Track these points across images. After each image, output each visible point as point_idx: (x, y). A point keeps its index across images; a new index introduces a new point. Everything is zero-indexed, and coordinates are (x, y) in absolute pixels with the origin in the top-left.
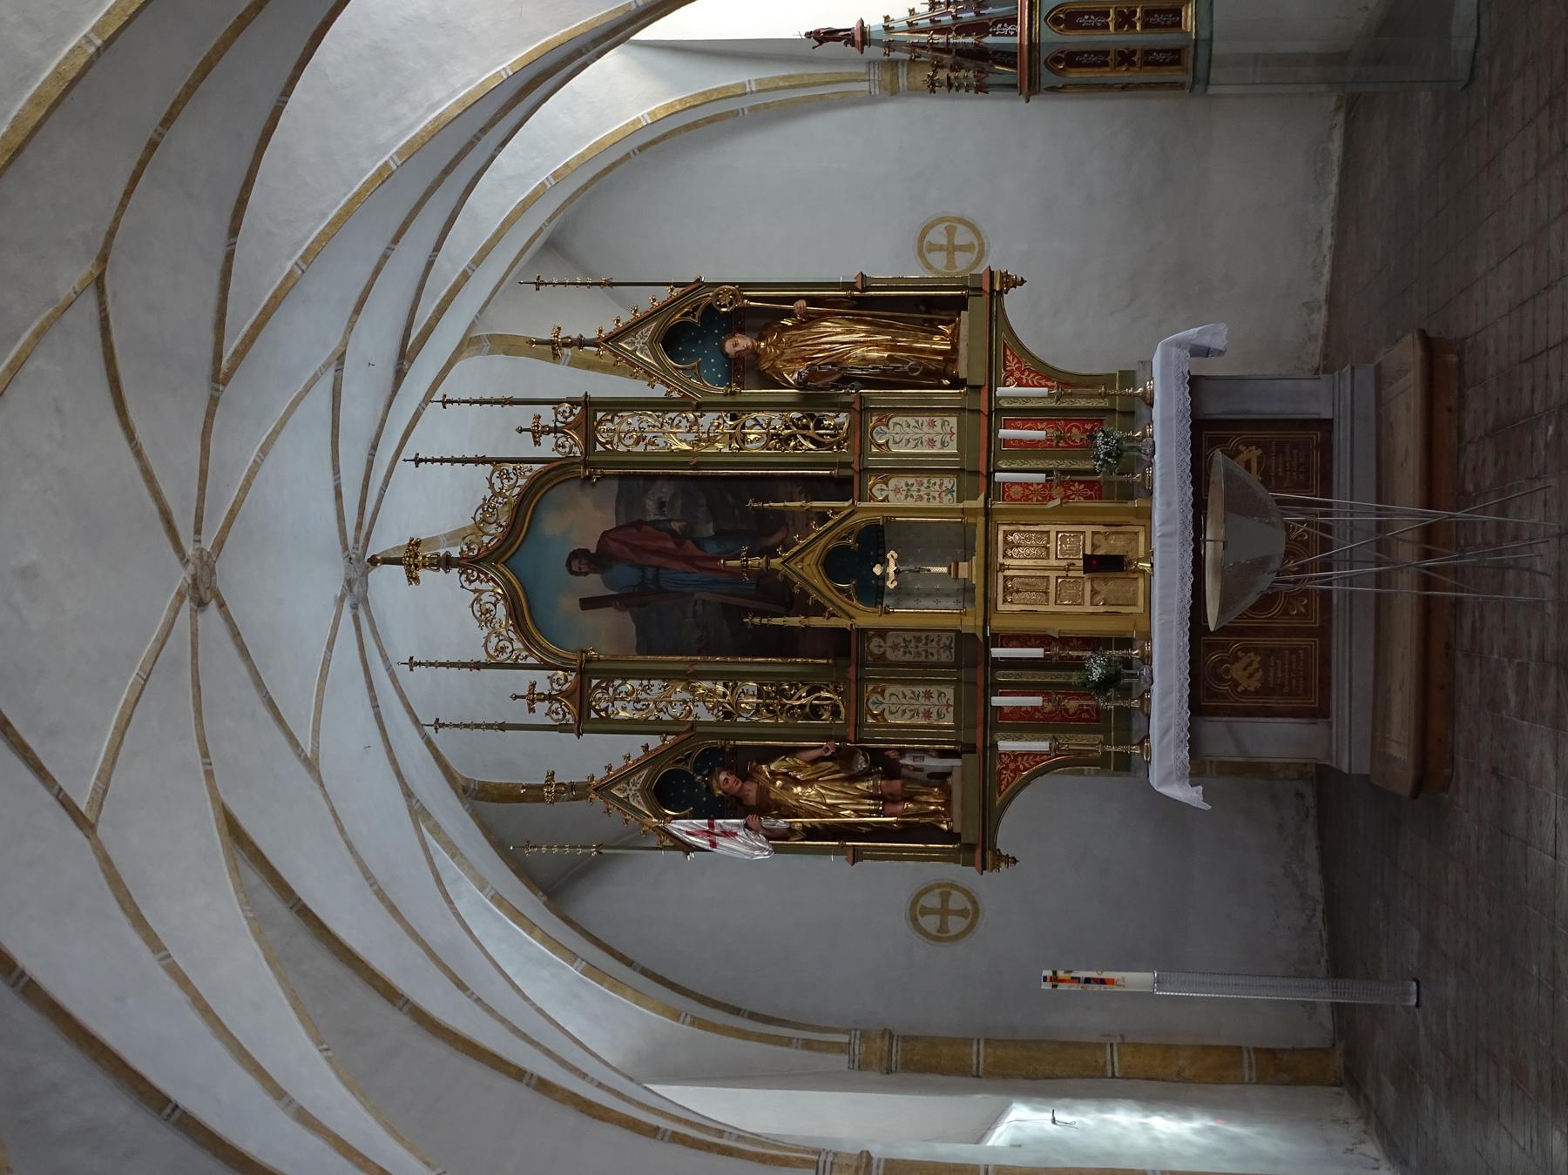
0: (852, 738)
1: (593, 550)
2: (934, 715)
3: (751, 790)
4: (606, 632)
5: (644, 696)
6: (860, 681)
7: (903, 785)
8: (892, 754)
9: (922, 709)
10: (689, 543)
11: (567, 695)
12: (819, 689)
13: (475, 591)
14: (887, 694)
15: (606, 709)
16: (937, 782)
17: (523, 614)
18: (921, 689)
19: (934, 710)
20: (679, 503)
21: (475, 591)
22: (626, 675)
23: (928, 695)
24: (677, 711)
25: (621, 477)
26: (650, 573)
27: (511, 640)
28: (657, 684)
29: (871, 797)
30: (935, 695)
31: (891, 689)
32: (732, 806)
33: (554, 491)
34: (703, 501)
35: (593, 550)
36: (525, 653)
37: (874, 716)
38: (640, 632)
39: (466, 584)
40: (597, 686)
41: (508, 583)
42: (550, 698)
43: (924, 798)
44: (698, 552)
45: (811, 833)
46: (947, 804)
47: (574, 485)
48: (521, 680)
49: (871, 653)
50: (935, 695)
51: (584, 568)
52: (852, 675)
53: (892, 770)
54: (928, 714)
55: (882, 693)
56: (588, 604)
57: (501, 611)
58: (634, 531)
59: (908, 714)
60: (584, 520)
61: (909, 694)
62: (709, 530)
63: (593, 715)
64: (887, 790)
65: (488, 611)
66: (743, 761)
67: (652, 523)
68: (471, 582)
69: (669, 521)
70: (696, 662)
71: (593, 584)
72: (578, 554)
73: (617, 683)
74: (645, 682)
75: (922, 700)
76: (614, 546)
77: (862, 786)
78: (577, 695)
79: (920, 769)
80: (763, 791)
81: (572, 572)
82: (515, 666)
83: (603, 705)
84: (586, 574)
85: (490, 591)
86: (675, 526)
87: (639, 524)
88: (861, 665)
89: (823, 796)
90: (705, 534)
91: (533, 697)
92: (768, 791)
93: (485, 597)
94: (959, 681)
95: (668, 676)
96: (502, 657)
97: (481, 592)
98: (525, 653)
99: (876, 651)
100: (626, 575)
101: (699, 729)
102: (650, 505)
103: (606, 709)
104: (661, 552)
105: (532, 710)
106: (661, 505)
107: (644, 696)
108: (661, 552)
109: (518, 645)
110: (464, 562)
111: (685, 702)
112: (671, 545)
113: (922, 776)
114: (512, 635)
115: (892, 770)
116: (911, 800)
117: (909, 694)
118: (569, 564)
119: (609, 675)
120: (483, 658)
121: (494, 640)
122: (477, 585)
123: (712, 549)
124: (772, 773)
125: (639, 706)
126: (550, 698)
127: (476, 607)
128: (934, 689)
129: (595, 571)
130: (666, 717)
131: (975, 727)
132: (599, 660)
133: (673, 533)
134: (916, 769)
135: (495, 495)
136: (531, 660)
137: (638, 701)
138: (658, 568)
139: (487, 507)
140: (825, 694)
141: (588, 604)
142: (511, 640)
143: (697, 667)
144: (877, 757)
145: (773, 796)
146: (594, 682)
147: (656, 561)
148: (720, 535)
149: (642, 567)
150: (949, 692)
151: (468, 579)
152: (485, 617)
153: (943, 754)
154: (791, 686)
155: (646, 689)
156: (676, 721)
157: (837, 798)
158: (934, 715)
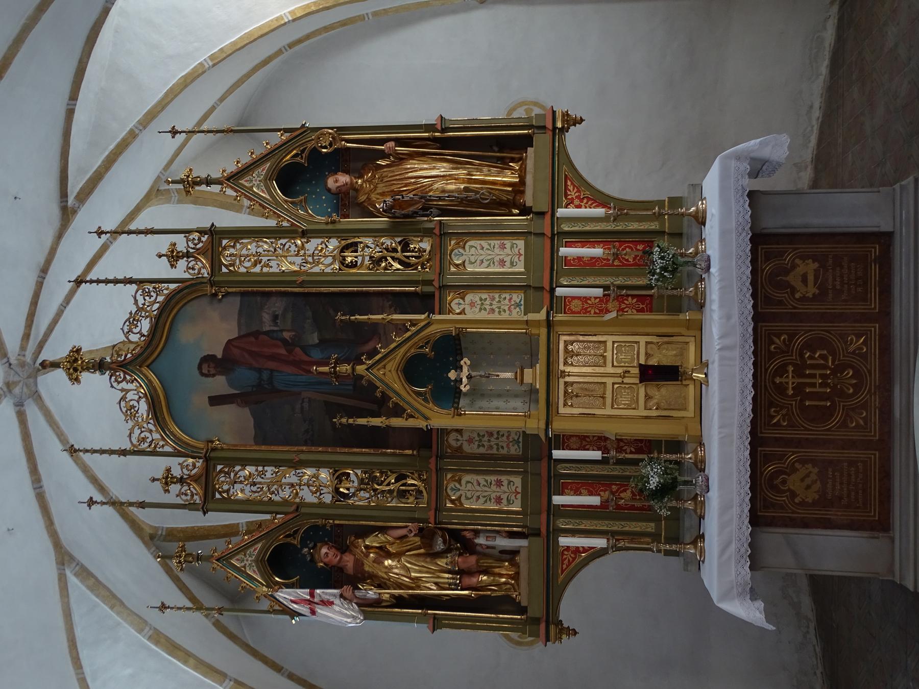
0: (432, 520)
1: (219, 356)
2: (505, 501)
3: (349, 561)
4: (230, 425)
5: (259, 479)
6: (440, 471)
7: (477, 561)
8: (468, 535)
9: (493, 495)
10: (298, 350)
11: (196, 479)
12: (404, 477)
13: (122, 390)
14: (463, 482)
15: (228, 491)
16: (508, 557)
17: (160, 409)
18: (493, 478)
19: (504, 497)
20: (289, 316)
21: (122, 390)
22: (244, 463)
23: (499, 483)
24: (286, 493)
25: (243, 294)
26: (265, 375)
27: (151, 431)
28: (270, 470)
29: (449, 572)
30: (505, 483)
31: (466, 478)
32: (332, 577)
33: (188, 307)
34: (309, 314)
35: (219, 356)
36: (161, 443)
37: (452, 501)
38: (258, 425)
39: (115, 384)
40: (221, 471)
41: (150, 384)
42: (181, 481)
43: (497, 570)
44: (305, 358)
45: (400, 602)
46: (516, 576)
47: (204, 301)
48: (158, 465)
49: (450, 446)
50: (505, 483)
51: (213, 371)
52: (432, 466)
53: (468, 547)
54: (499, 500)
55: (459, 481)
56: (215, 401)
57: (143, 407)
58: (252, 339)
59: (482, 500)
60: (211, 330)
61: (483, 482)
62: (314, 338)
63: (218, 496)
64: (463, 566)
65: (133, 407)
66: (342, 536)
67: (267, 333)
68: (119, 383)
69: (282, 331)
70: (302, 452)
71: (220, 384)
72: (208, 359)
73: (238, 468)
74: (260, 468)
75: (494, 488)
76: (236, 351)
77: (442, 562)
78: (203, 478)
79: (493, 548)
80: (359, 564)
81: (202, 374)
82: (154, 453)
83: (226, 487)
84: (214, 375)
85: (135, 389)
86: (286, 335)
87: (256, 334)
88: (440, 457)
89: (408, 570)
90: (311, 343)
91: (168, 480)
92: (363, 564)
93: (130, 396)
94: (526, 472)
95: (277, 463)
96: (144, 446)
97: (127, 391)
98: (161, 443)
99: (453, 443)
100: (245, 376)
101: (303, 510)
102: (266, 317)
103: (228, 491)
104: (273, 357)
105: (167, 491)
106: (275, 318)
107: (259, 479)
108: (273, 357)
109: (156, 436)
110: (114, 366)
111: (292, 485)
112: (283, 351)
113: (495, 552)
114: (151, 427)
115: (468, 547)
116: (486, 572)
117: (483, 482)
118: (200, 367)
119: (231, 462)
120: (128, 446)
121: (137, 431)
122: (124, 385)
123: (316, 355)
124: (367, 547)
125: (254, 489)
126: (181, 481)
127: (123, 404)
128: (504, 478)
129: (220, 373)
130: (276, 498)
131: (540, 514)
132: (222, 449)
133: (285, 342)
134: (488, 547)
135: (139, 310)
136: (168, 449)
137: (254, 484)
138: (272, 371)
139: (133, 320)
140: (410, 482)
141: (215, 401)
142: (151, 431)
143: (303, 457)
144: (455, 535)
145: (367, 569)
146: (219, 467)
147: (272, 365)
148: (323, 343)
149: (259, 371)
150: (518, 481)
151: (116, 380)
152: (130, 412)
153: (512, 535)
154: (382, 473)
155: (262, 474)
156: (285, 502)
157: (420, 572)
158: (505, 501)
